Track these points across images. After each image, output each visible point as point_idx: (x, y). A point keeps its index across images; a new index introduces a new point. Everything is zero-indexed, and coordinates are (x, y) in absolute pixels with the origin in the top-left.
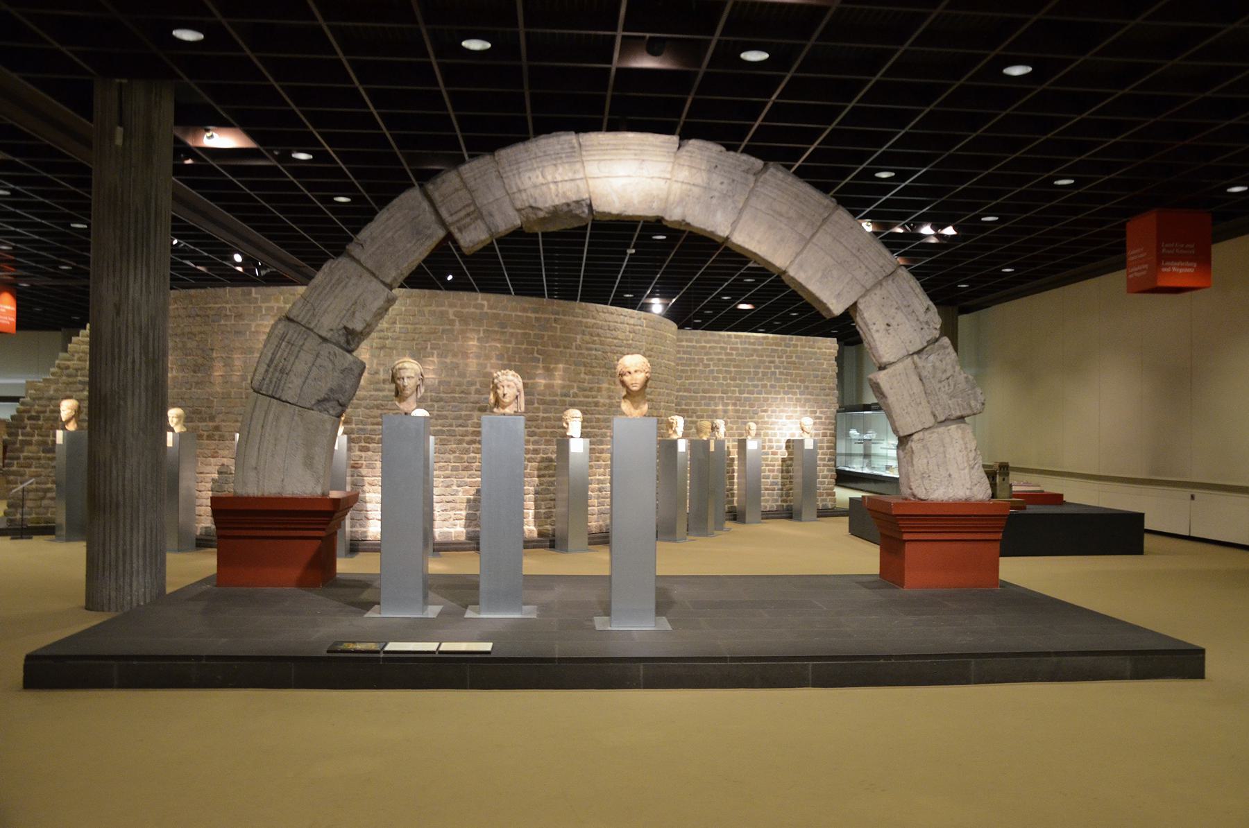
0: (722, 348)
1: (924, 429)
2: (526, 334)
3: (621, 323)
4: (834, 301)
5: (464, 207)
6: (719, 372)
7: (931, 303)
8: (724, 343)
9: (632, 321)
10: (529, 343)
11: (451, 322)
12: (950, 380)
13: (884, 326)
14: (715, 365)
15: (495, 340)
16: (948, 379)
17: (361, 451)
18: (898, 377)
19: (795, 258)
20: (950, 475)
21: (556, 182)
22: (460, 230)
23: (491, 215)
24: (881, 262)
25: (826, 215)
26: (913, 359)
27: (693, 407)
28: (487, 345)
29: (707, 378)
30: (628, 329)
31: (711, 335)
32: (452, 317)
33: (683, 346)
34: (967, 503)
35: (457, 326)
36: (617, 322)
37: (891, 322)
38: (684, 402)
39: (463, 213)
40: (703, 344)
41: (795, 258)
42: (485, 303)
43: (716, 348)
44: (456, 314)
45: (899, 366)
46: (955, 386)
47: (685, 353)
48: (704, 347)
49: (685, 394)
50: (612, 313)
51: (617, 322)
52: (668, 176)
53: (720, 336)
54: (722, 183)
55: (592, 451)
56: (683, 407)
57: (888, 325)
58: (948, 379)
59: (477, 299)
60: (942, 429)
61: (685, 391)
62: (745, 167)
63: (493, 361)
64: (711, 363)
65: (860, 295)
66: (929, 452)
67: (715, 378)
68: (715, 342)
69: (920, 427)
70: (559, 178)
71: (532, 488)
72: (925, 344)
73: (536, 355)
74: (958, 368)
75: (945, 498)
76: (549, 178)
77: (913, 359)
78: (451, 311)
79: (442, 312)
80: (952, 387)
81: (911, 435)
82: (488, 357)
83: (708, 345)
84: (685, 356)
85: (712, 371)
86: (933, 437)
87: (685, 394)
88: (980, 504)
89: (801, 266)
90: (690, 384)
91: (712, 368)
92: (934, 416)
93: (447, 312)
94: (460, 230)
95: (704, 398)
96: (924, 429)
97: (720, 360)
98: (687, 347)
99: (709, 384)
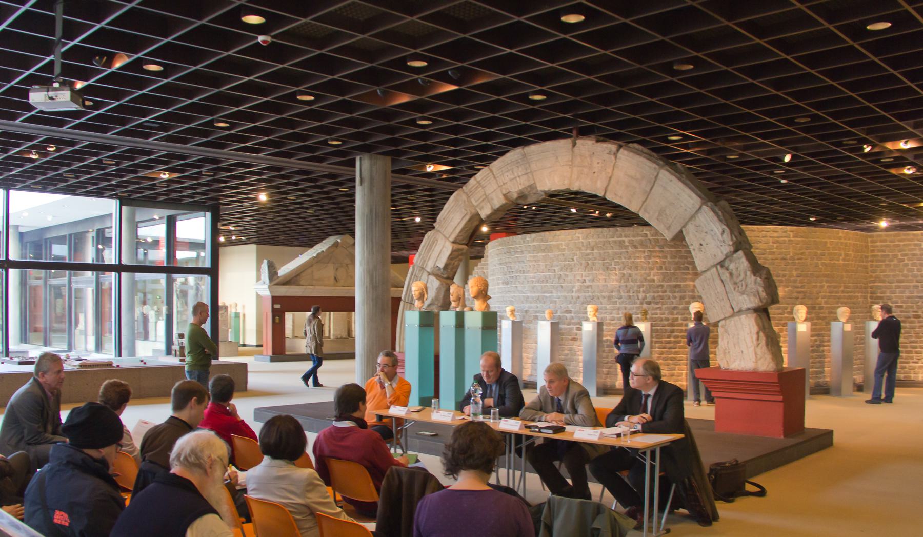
0: (916, 245)
1: (725, 319)
2: (677, 251)
3: (763, 237)
4: (666, 231)
5: (481, 197)
6: (914, 264)
7: (725, 227)
8: (919, 240)
9: (776, 235)
10: (681, 257)
11: (626, 247)
12: (743, 282)
13: (698, 246)
14: (909, 260)
15: (654, 257)
16: (741, 281)
17: (577, 330)
18: (708, 281)
19: (642, 205)
20: (742, 352)
21: (519, 176)
22: (481, 210)
23: (492, 199)
24: (692, 201)
25: (656, 174)
26: (717, 268)
27: (888, 295)
28: (650, 261)
29: (901, 271)
30: (771, 241)
31: (905, 235)
32: (627, 244)
33: (877, 246)
34: (754, 373)
35: (630, 249)
36: (758, 237)
37: (702, 243)
38: (879, 291)
39: (481, 200)
40: (897, 243)
41: (642, 205)
42: (648, 233)
43: (910, 245)
44: (629, 242)
45: (708, 274)
46: (746, 286)
47: (879, 251)
48: (898, 246)
49: (880, 284)
50: (752, 231)
51: (758, 237)
52: (570, 163)
53: (914, 235)
54: (598, 163)
55: (652, 330)
56: (879, 295)
57: (701, 245)
58: (741, 281)
59: (642, 231)
60: (736, 318)
61: (880, 282)
62: (607, 151)
63: (655, 271)
64: (905, 258)
65: (682, 225)
66: (729, 335)
67: (909, 271)
68: (909, 240)
69: (722, 317)
70: (520, 174)
71: (685, 356)
72: (724, 257)
73: (686, 265)
74: (749, 273)
75: (740, 368)
76: (516, 174)
77: (717, 268)
78: (626, 240)
79: (620, 242)
80: (744, 287)
81: (719, 322)
82: (651, 269)
83: (902, 243)
84: (880, 254)
85: (906, 265)
86: (732, 322)
87: (880, 284)
88: (765, 374)
89: (645, 211)
90: (885, 276)
91: (906, 262)
92: (733, 309)
93: (624, 241)
94: (481, 210)
95: (899, 287)
96: (725, 319)
97: (914, 255)
98: (882, 246)
99: (903, 276)
